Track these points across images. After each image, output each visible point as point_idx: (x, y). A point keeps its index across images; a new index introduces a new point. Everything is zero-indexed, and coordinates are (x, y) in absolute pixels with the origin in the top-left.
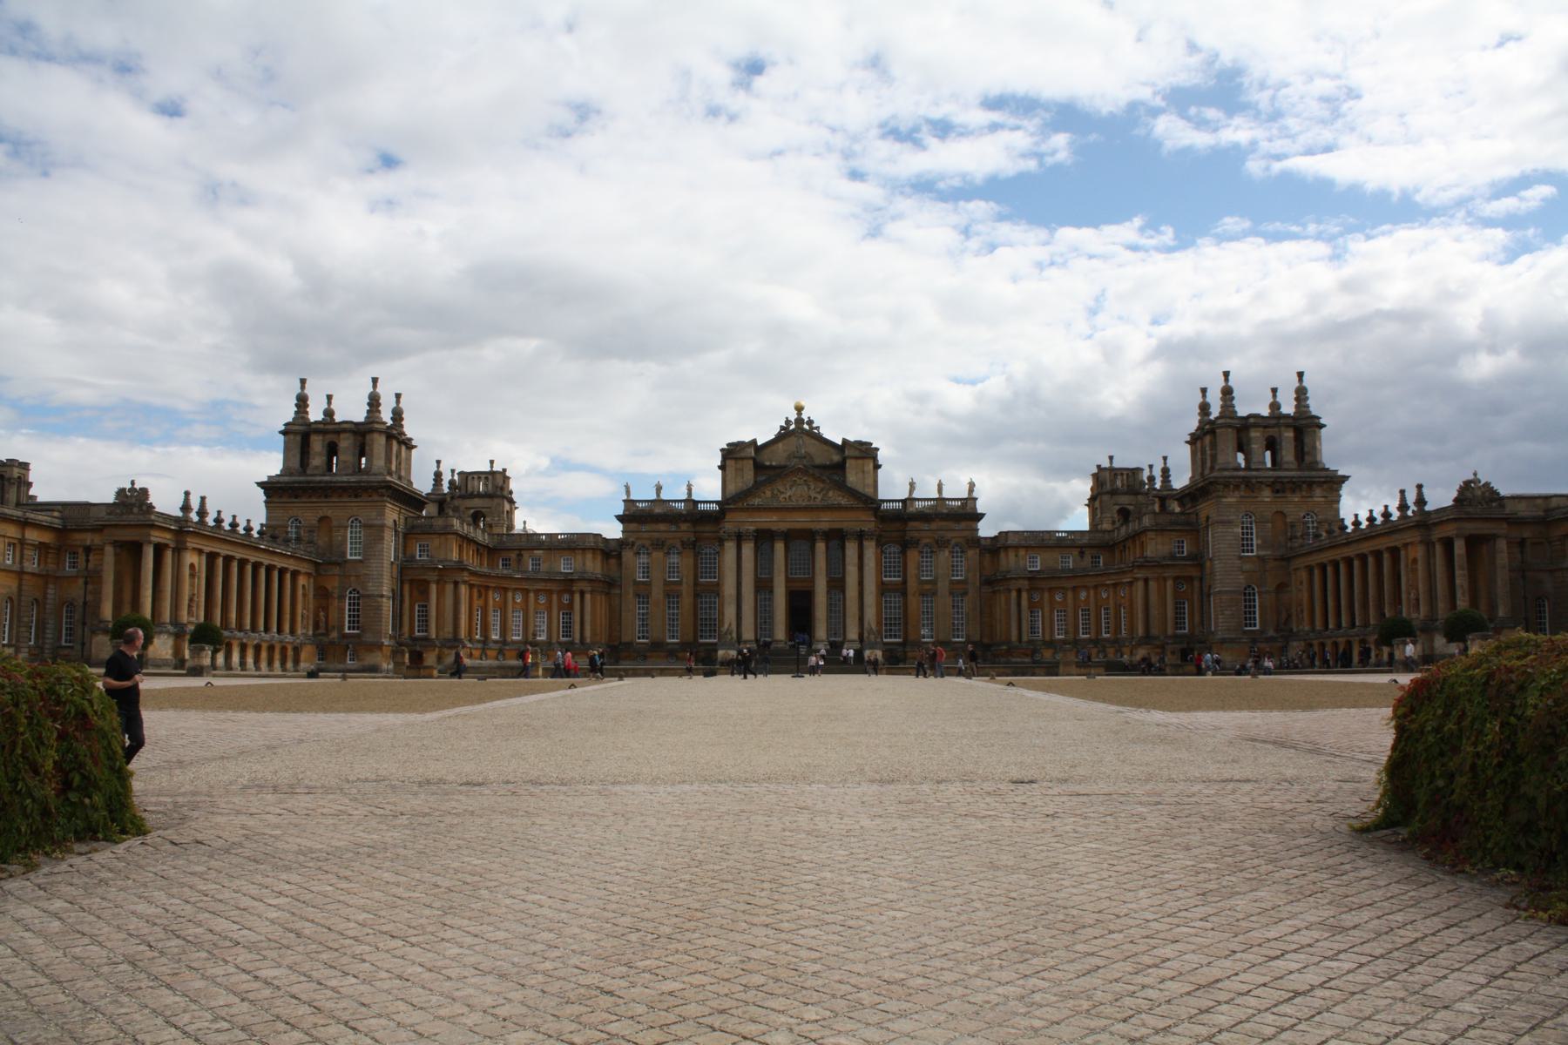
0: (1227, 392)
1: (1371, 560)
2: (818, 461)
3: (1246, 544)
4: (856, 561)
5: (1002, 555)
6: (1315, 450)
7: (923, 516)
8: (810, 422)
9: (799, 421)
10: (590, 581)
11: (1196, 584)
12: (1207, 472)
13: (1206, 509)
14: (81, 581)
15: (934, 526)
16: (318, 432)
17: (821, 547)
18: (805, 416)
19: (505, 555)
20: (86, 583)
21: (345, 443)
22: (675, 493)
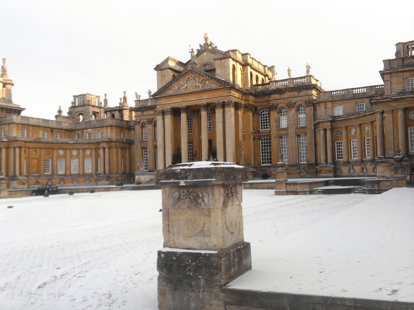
4: (221, 120)
7: (279, 91)
8: (211, 44)
9: (206, 44)
10: (107, 142)
15: (285, 95)
17: (204, 114)
19: (77, 132)
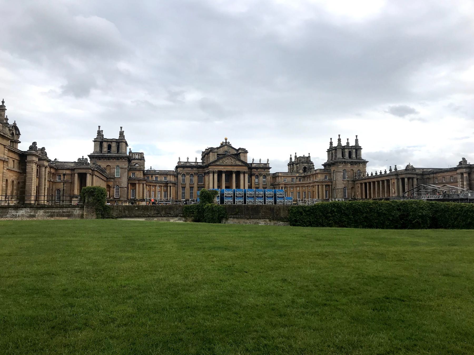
0: (339, 140)
1: (381, 182)
2: (231, 153)
3: (344, 177)
5: (277, 178)
6: (360, 154)
8: (229, 143)
11: (331, 187)
12: (333, 159)
13: (333, 169)
14: (62, 183)
15: (259, 170)
16: (105, 141)
17: (234, 175)
18: (228, 141)
20: (64, 184)
21: (114, 145)
22: (192, 160)
